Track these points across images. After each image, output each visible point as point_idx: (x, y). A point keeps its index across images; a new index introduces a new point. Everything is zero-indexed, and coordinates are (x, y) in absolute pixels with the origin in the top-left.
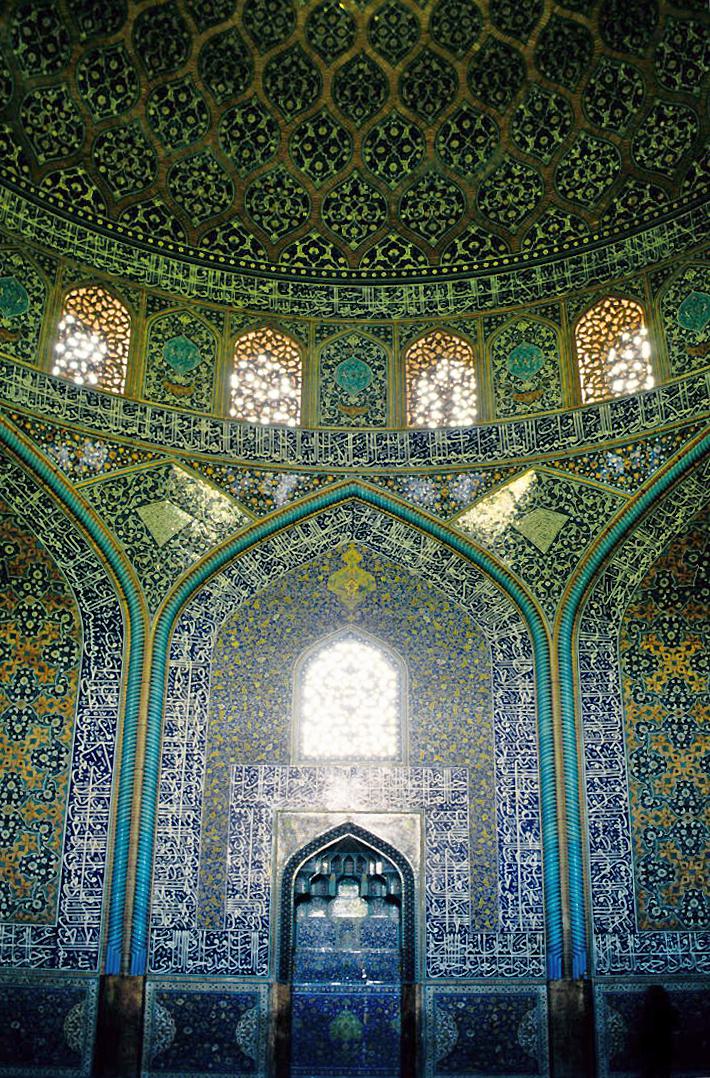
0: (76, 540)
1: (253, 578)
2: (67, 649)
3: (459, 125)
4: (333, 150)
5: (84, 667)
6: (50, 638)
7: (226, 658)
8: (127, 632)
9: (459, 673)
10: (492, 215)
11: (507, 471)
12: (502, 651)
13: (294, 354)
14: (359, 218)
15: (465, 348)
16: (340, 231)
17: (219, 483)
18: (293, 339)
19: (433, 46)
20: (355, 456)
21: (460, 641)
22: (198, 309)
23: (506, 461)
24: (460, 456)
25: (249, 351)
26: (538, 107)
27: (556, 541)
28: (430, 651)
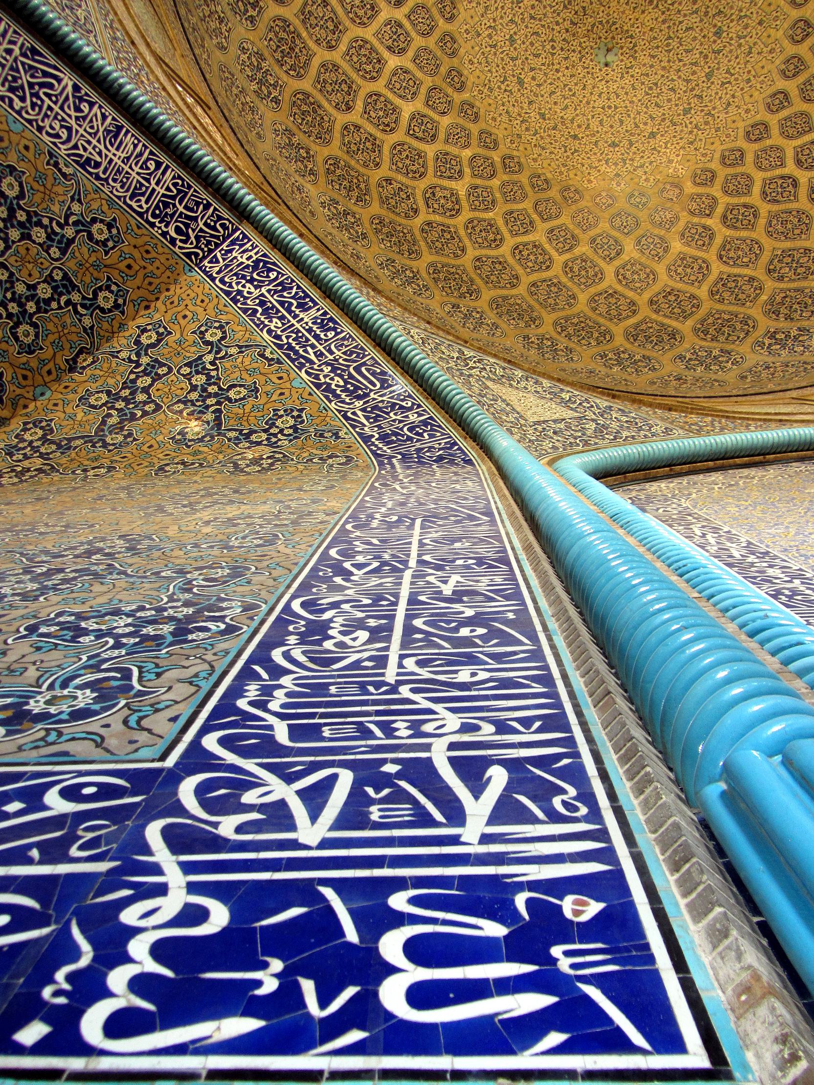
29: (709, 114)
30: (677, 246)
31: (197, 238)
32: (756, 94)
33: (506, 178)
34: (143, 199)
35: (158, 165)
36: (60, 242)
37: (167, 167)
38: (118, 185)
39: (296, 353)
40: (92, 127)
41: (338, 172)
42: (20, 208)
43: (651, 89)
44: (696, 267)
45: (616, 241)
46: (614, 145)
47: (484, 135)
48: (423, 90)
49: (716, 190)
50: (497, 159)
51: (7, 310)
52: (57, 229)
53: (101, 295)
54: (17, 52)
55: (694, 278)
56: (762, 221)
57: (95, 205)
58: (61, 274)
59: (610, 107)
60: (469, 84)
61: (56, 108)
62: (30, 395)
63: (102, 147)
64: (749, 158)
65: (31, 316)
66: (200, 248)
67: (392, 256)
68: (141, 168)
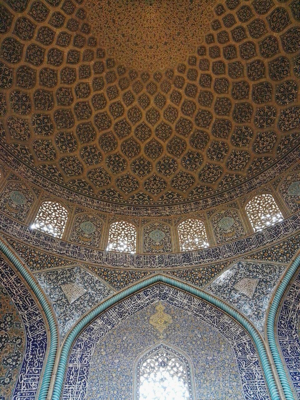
0: (30, 300)
1: (114, 320)
2: (16, 358)
3: (189, 156)
4: (146, 168)
5: (23, 367)
6: (8, 353)
7: (98, 361)
8: (48, 348)
9: (220, 364)
10: (205, 181)
11: (226, 263)
12: (240, 351)
13: (133, 229)
14: (157, 187)
15: (200, 222)
16: (150, 191)
17: (100, 275)
18: (133, 224)
19: (177, 135)
20: (159, 264)
21: (218, 346)
22: (96, 213)
23: (226, 259)
24: (205, 260)
25: (116, 228)
26: (216, 146)
27: (256, 292)
28: (203, 352)
29: (186, 37)
30: (169, 102)
32: (203, 33)
33: (108, 70)
39: (11, 291)
41: (40, 97)
43: (166, 19)
44: (173, 113)
45: (148, 98)
46: (151, 47)
47: (99, 52)
48: (72, 39)
49: (185, 76)
50: (105, 62)
55: (172, 118)
56: (198, 94)
59: (151, 27)
60: (92, 29)
64: (198, 63)
67: (62, 131)
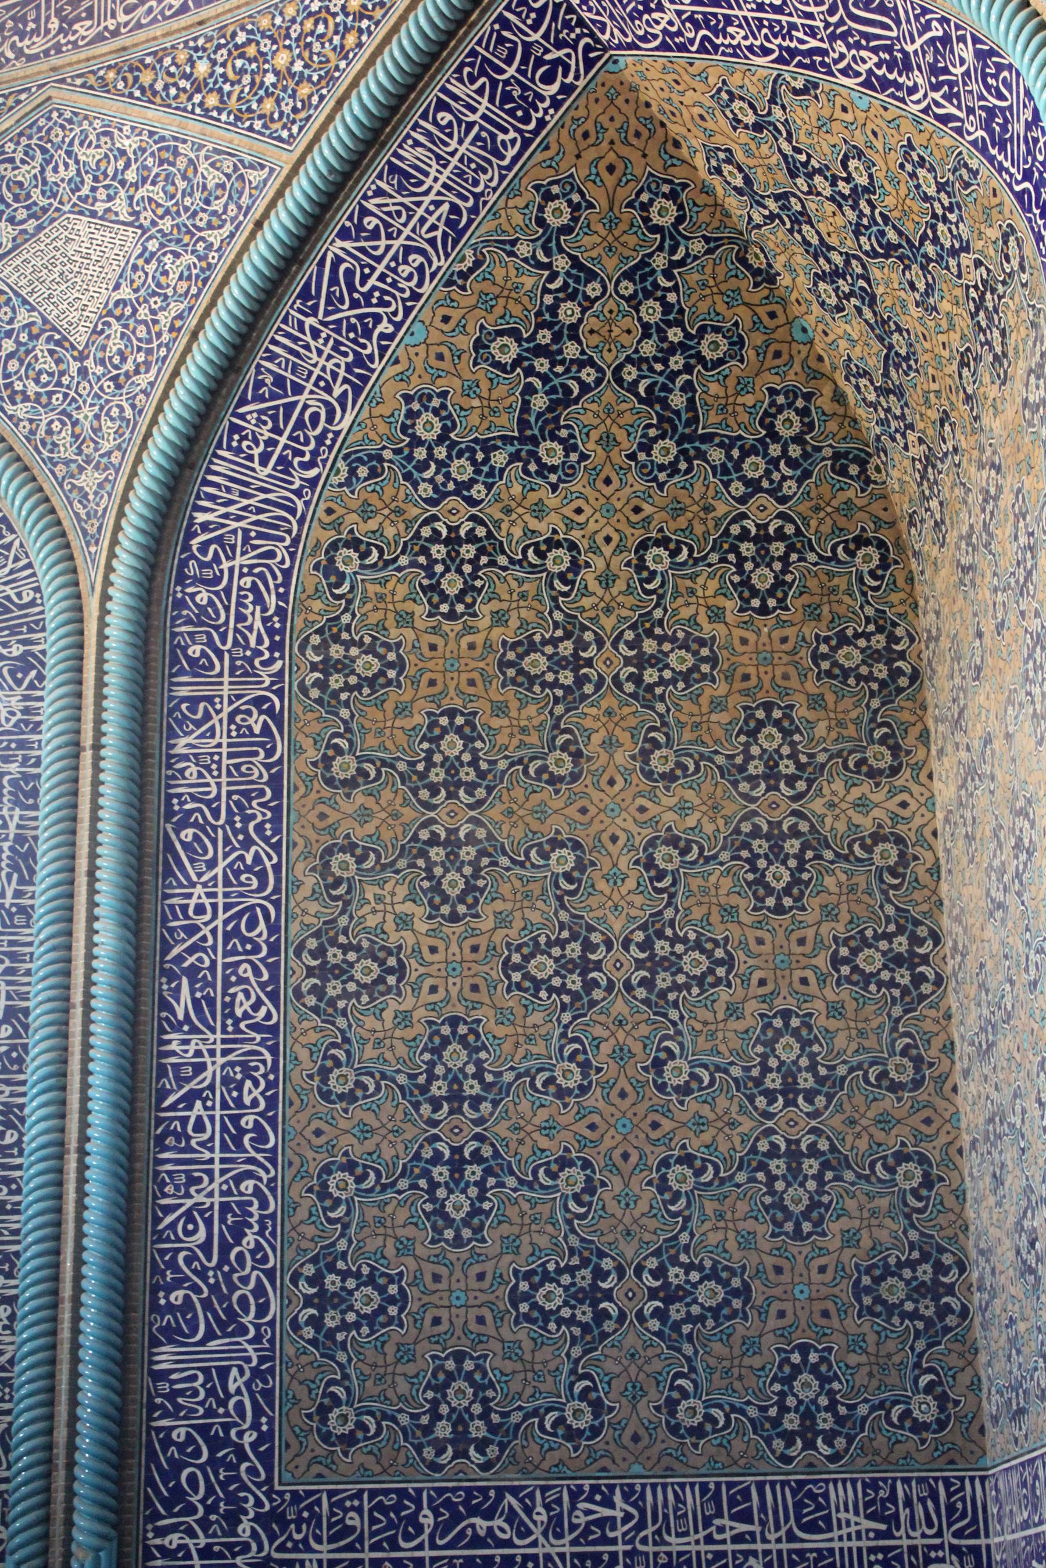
31: (559, 45)
34: (501, 136)
35: (441, 106)
36: (577, 280)
37: (444, 90)
38: (483, 178)
40: (399, 214)
42: (532, 338)
51: (679, 373)
52: (558, 284)
53: (656, 220)
54: (310, 321)
57: (518, 219)
58: (625, 283)
61: (381, 268)
62: (804, 349)
63: (427, 200)
65: (688, 336)
66: (577, 41)
68: (450, 135)
